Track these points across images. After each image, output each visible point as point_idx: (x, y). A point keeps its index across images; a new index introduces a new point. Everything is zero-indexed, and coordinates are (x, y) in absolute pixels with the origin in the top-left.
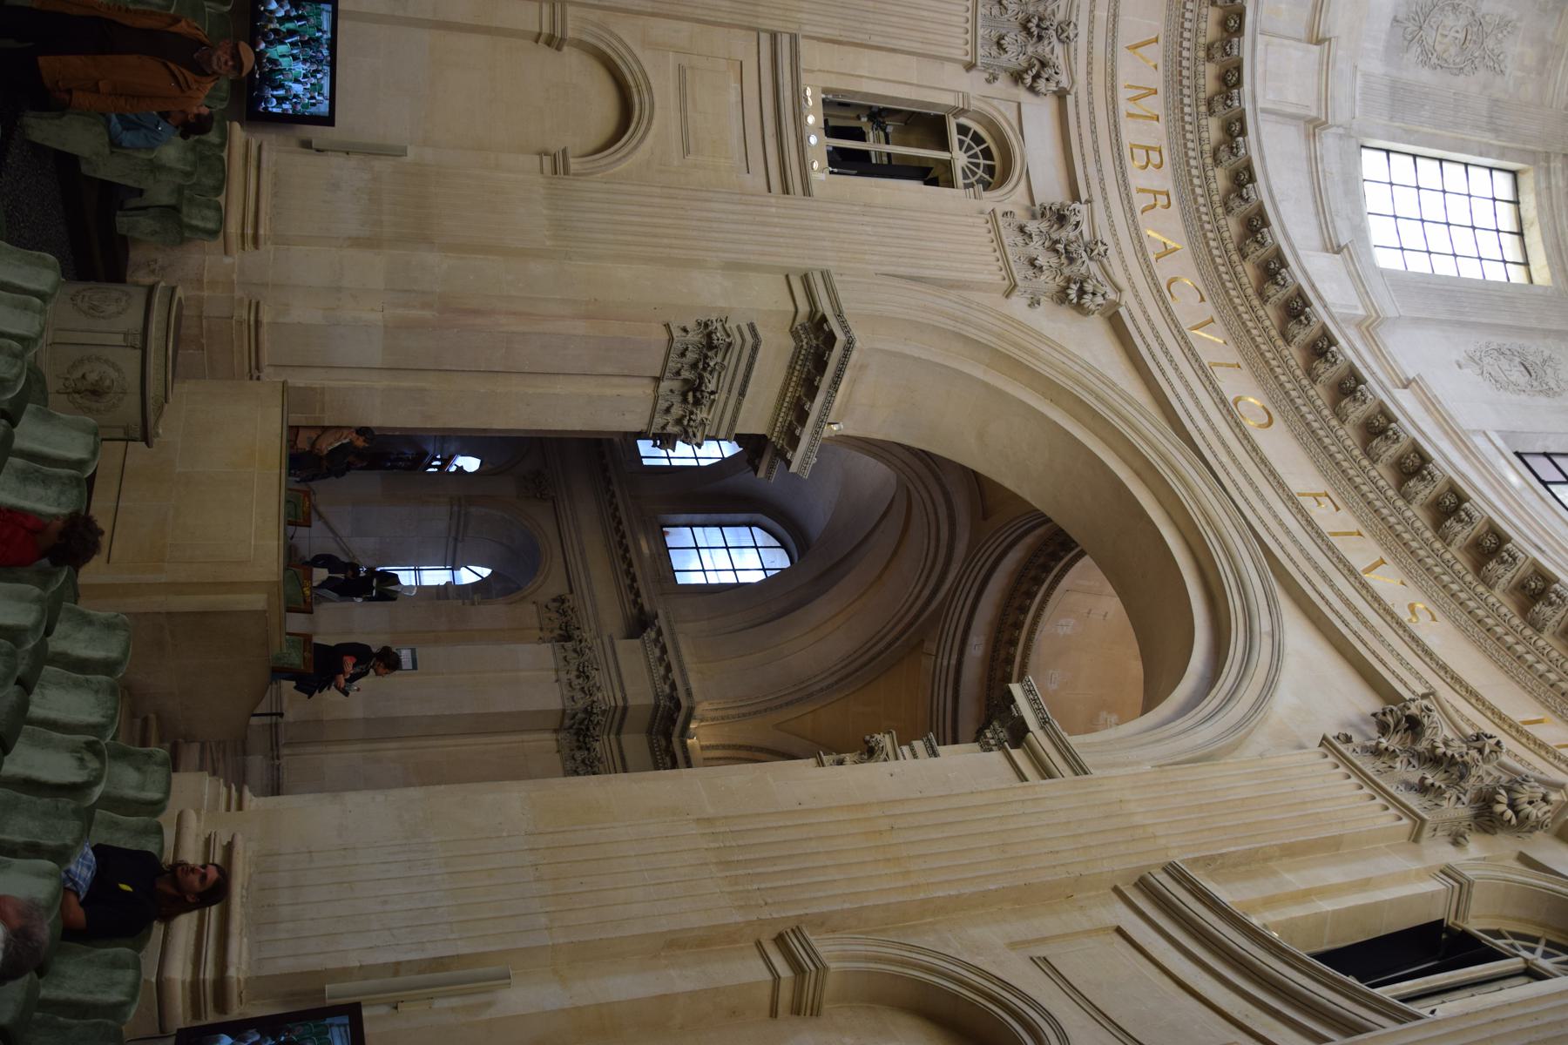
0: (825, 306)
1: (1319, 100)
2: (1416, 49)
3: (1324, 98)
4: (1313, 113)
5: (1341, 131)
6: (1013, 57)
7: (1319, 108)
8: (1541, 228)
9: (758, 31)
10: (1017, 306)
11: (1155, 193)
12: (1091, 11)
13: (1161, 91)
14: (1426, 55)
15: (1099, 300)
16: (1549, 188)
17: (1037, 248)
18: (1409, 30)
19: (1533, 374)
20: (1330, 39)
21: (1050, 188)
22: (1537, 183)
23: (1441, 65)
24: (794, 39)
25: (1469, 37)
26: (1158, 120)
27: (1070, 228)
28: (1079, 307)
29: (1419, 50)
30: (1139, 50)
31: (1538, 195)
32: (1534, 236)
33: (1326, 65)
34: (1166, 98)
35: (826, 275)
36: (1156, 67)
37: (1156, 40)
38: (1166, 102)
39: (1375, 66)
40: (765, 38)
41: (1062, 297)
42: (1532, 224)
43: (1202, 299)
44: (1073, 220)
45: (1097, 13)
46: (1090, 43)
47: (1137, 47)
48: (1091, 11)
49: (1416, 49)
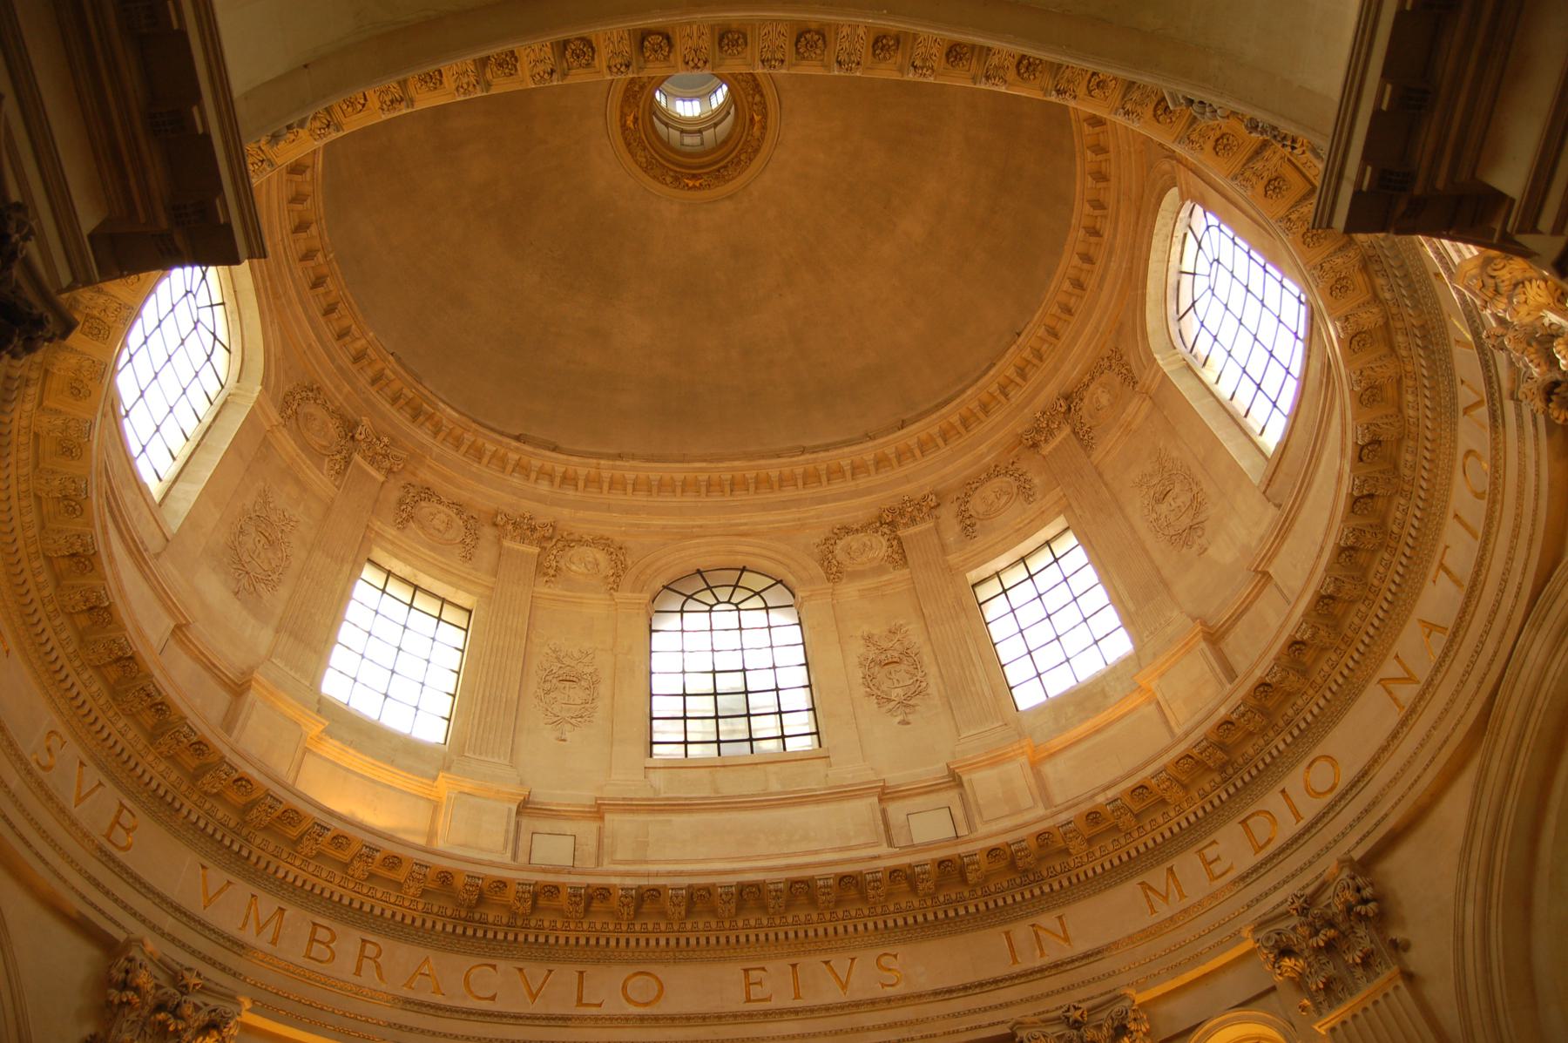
2: (261, 587)
8: (424, 572)
11: (362, 956)
16: (393, 543)
18: (246, 584)
19: (574, 679)
22: (387, 551)
25: (267, 534)
29: (263, 585)
31: (396, 556)
32: (425, 581)
38: (269, 892)
42: (415, 576)
43: (494, 967)
45: (167, 929)
49: (261, 587)
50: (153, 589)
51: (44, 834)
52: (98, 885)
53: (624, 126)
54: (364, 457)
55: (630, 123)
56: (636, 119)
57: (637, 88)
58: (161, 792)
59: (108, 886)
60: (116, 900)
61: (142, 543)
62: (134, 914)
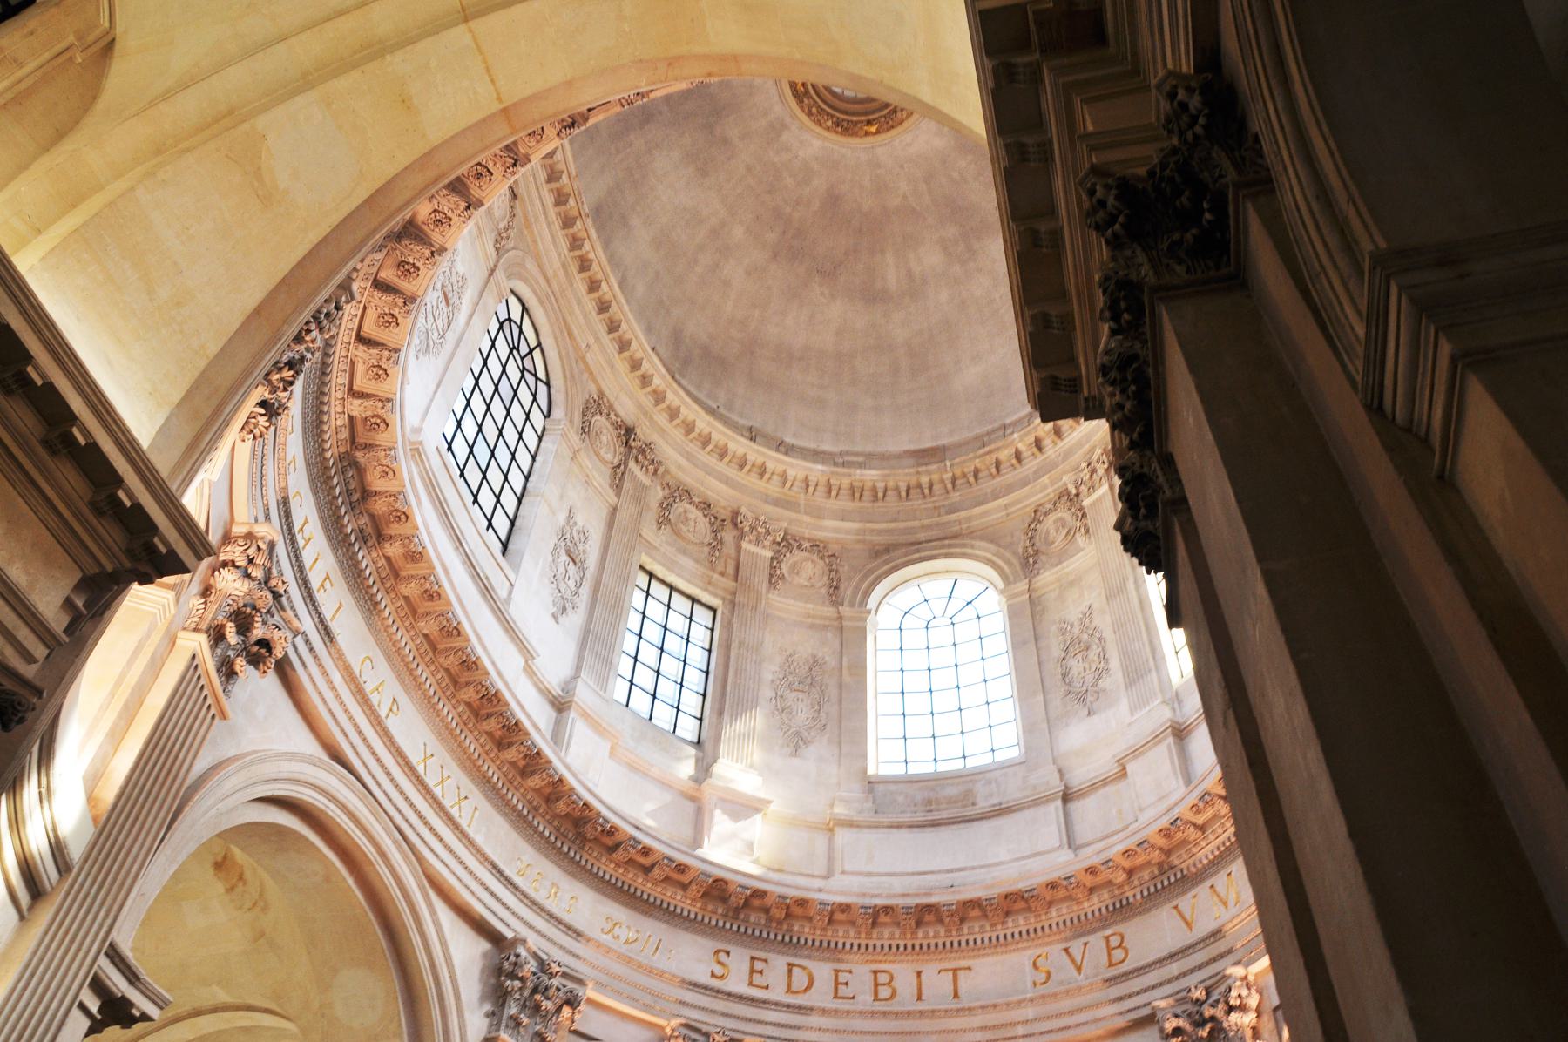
1: (1160, 742)
3: (1156, 739)
4: (1170, 740)
5: (1176, 705)
7: (1165, 738)
12: (1177, 978)
13: (1208, 883)
14: (1100, 674)
20: (1118, 761)
23: (1104, 657)
26: (1230, 874)
30: (1188, 918)
33: (1136, 752)
34: (1212, 875)
36: (1195, 897)
37: (1176, 907)
38: (1215, 873)
39: (1123, 706)
45: (1176, 973)
46: (1200, 967)
47: (1188, 924)
48: (1177, 978)
50: (1030, 807)
51: (1071, 1013)
52: (1121, 999)
53: (878, 132)
54: (1089, 494)
55: (873, 129)
56: (869, 123)
57: (839, 129)
58: (1111, 908)
59: (1128, 992)
60: (1138, 993)
61: (994, 805)
62: (1154, 987)
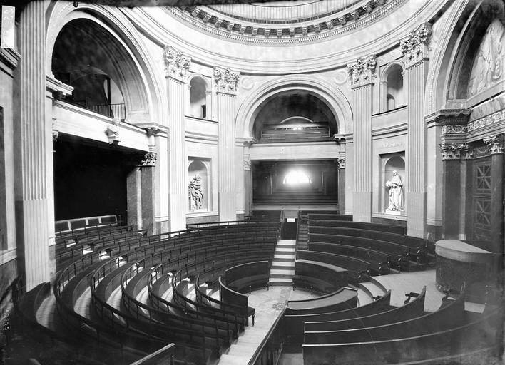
0: (433, 118)
6: (369, 73)
9: (372, 140)
10: (431, 55)
15: (425, 30)
17: (414, 53)
21: (398, 52)
24: (372, 132)
27: (407, 45)
28: (430, 34)
35: (426, 118)
40: (374, 138)
41: (427, 43)
44: (405, 44)
